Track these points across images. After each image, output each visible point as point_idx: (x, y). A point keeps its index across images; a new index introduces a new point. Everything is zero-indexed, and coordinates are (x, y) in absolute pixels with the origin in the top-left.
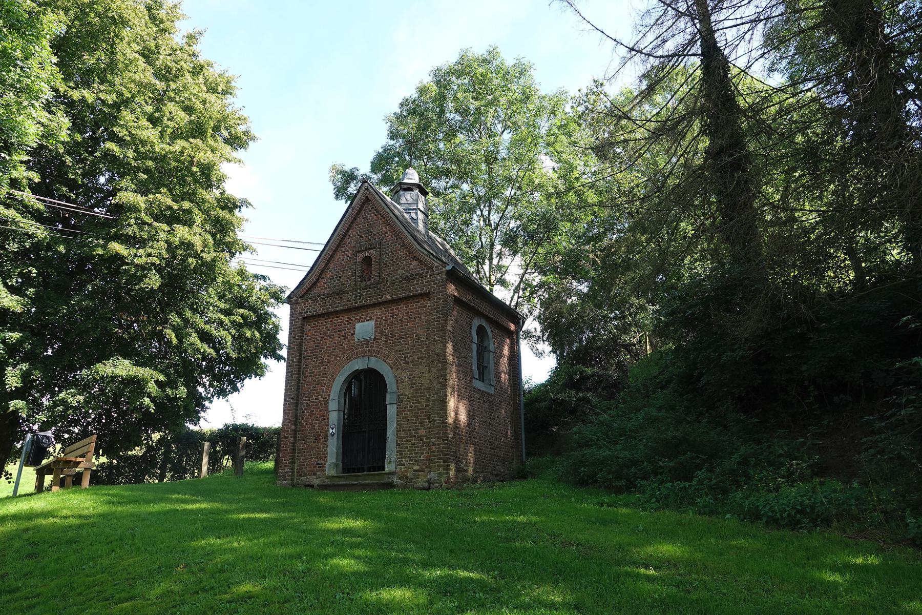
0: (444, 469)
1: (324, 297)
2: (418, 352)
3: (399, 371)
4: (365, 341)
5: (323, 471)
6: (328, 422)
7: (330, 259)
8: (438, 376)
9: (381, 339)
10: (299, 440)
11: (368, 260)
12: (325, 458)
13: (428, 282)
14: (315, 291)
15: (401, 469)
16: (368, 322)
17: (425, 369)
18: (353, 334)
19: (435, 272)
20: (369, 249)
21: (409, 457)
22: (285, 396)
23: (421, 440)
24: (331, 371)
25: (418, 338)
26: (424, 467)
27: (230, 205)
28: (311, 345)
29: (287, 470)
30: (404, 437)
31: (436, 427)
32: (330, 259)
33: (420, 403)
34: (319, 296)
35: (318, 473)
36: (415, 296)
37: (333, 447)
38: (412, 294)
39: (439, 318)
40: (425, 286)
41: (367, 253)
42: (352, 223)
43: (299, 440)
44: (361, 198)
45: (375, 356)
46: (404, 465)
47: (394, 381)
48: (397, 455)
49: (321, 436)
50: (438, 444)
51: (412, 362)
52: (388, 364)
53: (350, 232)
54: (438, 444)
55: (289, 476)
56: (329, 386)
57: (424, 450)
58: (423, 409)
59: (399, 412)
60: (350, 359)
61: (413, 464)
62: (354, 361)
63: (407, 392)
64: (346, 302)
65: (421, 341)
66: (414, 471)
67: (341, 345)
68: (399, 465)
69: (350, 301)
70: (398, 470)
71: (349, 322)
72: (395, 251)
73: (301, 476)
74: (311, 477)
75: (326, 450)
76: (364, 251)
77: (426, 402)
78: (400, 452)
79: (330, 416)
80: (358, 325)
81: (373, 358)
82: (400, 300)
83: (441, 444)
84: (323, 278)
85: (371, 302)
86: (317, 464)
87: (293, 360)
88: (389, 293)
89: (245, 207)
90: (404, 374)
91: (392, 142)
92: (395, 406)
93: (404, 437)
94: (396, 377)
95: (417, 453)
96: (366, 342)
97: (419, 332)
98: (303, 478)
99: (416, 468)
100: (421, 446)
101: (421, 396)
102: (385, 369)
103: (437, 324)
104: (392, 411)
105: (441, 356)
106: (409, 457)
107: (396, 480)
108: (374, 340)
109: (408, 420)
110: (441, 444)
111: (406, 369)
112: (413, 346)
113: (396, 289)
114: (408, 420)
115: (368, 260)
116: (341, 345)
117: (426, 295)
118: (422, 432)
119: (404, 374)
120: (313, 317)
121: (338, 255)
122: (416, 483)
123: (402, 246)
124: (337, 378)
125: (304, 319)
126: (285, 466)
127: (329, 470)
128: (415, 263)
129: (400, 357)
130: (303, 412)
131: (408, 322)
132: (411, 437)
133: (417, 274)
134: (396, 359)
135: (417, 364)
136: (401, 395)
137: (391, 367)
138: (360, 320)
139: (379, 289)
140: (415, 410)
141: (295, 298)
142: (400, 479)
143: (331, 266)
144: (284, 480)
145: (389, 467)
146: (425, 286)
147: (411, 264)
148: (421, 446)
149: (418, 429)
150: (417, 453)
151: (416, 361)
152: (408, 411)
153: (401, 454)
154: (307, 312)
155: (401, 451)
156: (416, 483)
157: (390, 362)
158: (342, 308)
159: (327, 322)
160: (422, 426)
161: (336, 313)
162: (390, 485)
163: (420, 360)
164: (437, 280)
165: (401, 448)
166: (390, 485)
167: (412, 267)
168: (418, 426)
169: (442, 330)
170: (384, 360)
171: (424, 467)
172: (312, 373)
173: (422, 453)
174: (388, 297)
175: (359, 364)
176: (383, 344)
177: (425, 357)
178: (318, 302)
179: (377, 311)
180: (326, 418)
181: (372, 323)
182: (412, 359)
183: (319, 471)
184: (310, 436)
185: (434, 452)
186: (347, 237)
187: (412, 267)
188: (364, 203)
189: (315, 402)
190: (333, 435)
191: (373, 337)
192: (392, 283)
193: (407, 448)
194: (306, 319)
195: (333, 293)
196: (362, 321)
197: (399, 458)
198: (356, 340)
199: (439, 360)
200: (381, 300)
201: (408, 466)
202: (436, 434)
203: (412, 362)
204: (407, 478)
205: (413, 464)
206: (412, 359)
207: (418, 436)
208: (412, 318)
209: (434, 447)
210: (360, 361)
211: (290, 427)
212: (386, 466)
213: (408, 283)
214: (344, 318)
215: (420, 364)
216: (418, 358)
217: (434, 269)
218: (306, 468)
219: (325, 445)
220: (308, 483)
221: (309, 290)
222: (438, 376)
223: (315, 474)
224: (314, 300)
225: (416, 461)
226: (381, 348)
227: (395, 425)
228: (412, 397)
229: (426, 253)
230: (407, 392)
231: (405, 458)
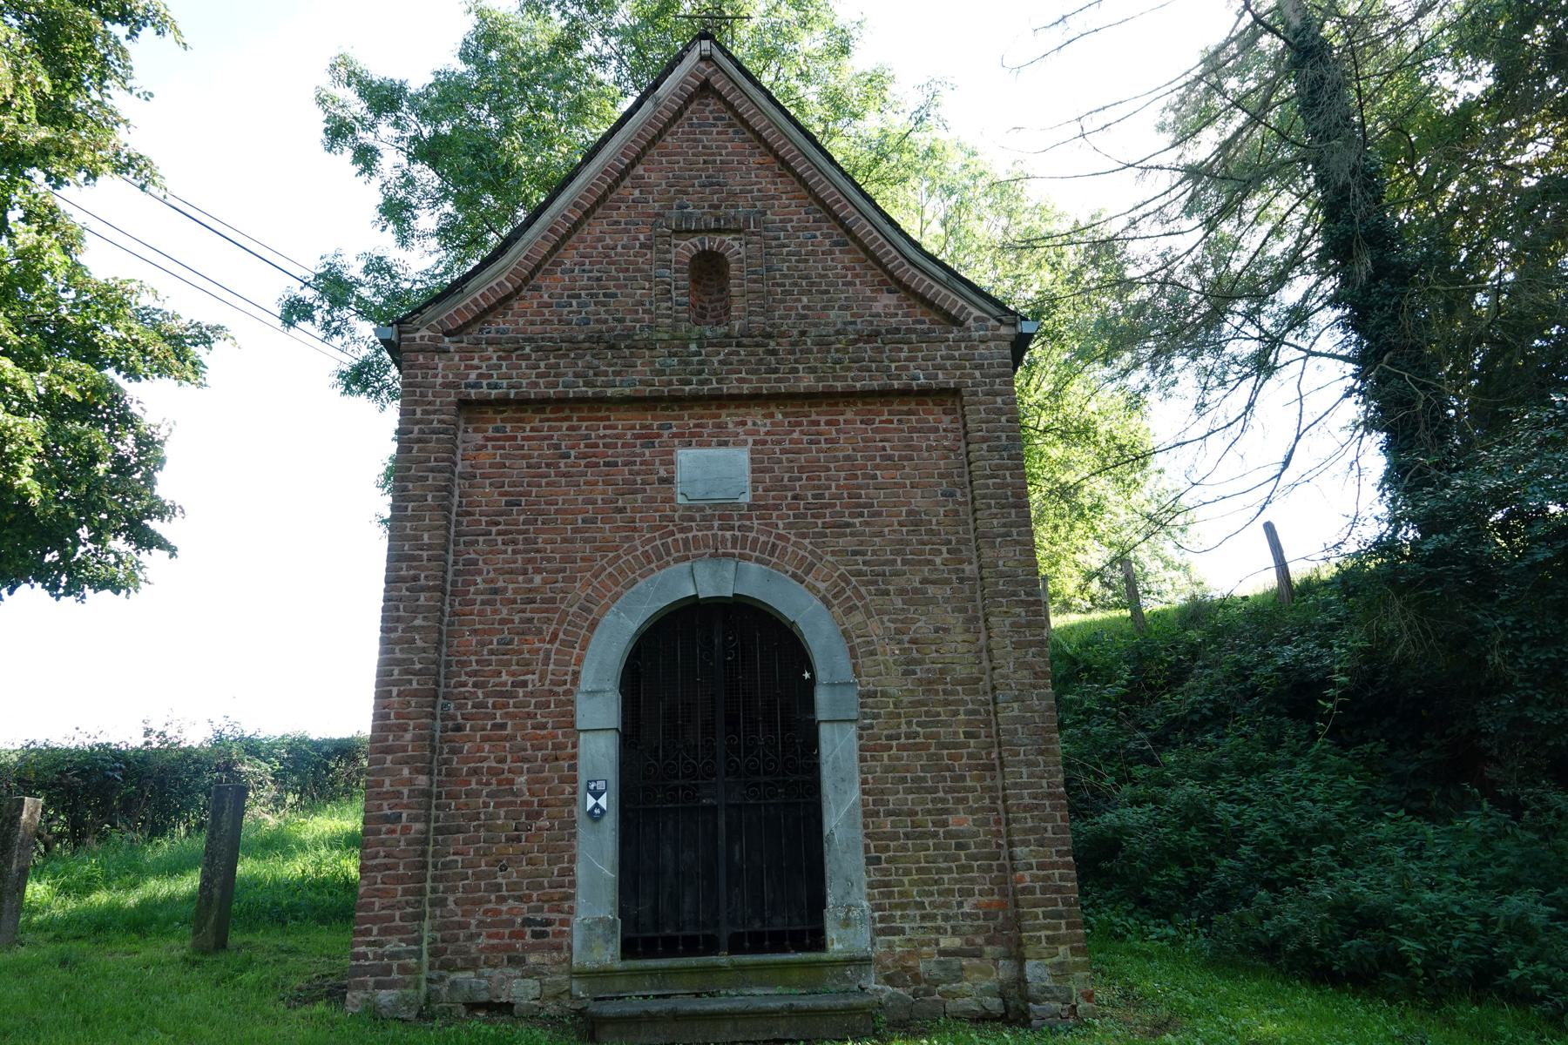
0: (1075, 951)
2: (919, 562)
3: (858, 617)
4: (714, 507)
5: (559, 948)
6: (573, 768)
7: (568, 235)
8: (1018, 645)
9: (776, 507)
10: (438, 831)
11: (709, 268)
12: (563, 895)
13: (952, 358)
14: (502, 324)
15: (890, 945)
16: (722, 451)
17: (954, 620)
18: (668, 481)
19: (975, 335)
20: (718, 231)
21: (921, 905)
23: (959, 847)
24: (579, 591)
25: (915, 520)
26: (979, 940)
28: (487, 495)
29: (394, 944)
30: (895, 836)
31: (1027, 808)
32: (568, 235)
33: (944, 724)
34: (530, 340)
35: (533, 959)
36: (905, 393)
38: (896, 384)
39: (999, 467)
40: (937, 367)
41: (712, 242)
42: (652, 143)
43: (438, 831)
44: (685, 81)
45: (758, 560)
46: (901, 931)
48: (870, 897)
50: (1041, 866)
51: (902, 592)
52: (813, 589)
53: (639, 170)
54: (1041, 866)
55: (404, 969)
56: (575, 642)
57: (972, 881)
58: (956, 746)
59: (869, 750)
60: (659, 558)
61: (938, 930)
62: (674, 567)
63: (894, 684)
64: (640, 376)
65: (931, 532)
66: (943, 953)
67: (621, 510)
68: (882, 932)
69: (661, 373)
71: (648, 439)
72: (813, 253)
73: (449, 966)
74: (497, 974)
75: (570, 871)
76: (697, 231)
77: (968, 723)
78: (882, 886)
79: (581, 750)
80: (686, 458)
81: (753, 566)
82: (850, 396)
83: (1053, 865)
84: (537, 288)
85: (746, 389)
86: (527, 922)
87: (418, 538)
88: (813, 370)
90: (874, 627)
92: (852, 730)
93: (895, 836)
94: (846, 634)
95: (950, 892)
96: (724, 512)
97: (918, 502)
98: (459, 976)
99: (945, 942)
101: (947, 703)
103: (997, 486)
105: (1023, 583)
106: (921, 905)
108: (751, 507)
109: (904, 780)
110: (1053, 865)
111: (880, 612)
112: (900, 542)
113: (839, 361)
114: (904, 780)
115: (709, 268)
116: (621, 510)
117: (947, 396)
118: (961, 821)
119: (874, 627)
120: (502, 403)
121: (594, 229)
122: (954, 995)
123: (836, 244)
124: (609, 617)
125: (464, 404)
126: (383, 932)
127: (587, 946)
129: (859, 573)
130: (459, 728)
131: (877, 467)
132: (922, 836)
133: (909, 331)
135: (915, 598)
136: (873, 694)
137: (824, 600)
138: (690, 439)
139: (774, 353)
140: (926, 747)
141: (425, 332)
142: (889, 980)
143: (569, 258)
144: (380, 985)
145: (838, 943)
146: (937, 367)
147: (875, 300)
148: (963, 869)
149: (946, 811)
150: (950, 892)
151: (915, 591)
152: (901, 748)
153: (890, 895)
154: (477, 385)
155: (887, 884)
156: (954, 995)
157: (822, 586)
158: (627, 391)
160: (959, 801)
161: (597, 404)
163: (931, 590)
164: (982, 357)
165: (886, 872)
167: (878, 307)
168: (943, 800)
169: (1015, 506)
170: (794, 576)
171: (979, 940)
172: (495, 591)
173: (970, 893)
174: (806, 382)
176: (789, 526)
177: (947, 582)
178: (528, 357)
179: (757, 419)
180: (564, 755)
181: (741, 457)
182: (901, 582)
183: (533, 949)
184: (491, 817)
185: (1031, 891)
186: (627, 182)
187: (878, 307)
188: (690, 99)
189: (512, 695)
190: (595, 816)
191: (746, 499)
192: (823, 344)
193: (907, 872)
194: (469, 407)
195: (589, 339)
196: (700, 445)
197: (878, 907)
198: (680, 499)
199: (1014, 594)
200: (783, 387)
201: (919, 936)
202: (1032, 830)
203: (902, 592)
204: (917, 978)
205: (938, 930)
206: (901, 582)
207: (948, 835)
208: (890, 458)
209: (1027, 875)
210: (703, 570)
211: (410, 782)
212: (832, 932)
214: (625, 425)
216: (924, 581)
217: (970, 322)
218: (471, 937)
219: (562, 848)
220: (484, 997)
221: (482, 316)
222: (1018, 645)
224: (511, 349)
225: (946, 918)
226: (779, 537)
227: (855, 795)
229: (942, 275)
230: (894, 684)
231: (903, 907)
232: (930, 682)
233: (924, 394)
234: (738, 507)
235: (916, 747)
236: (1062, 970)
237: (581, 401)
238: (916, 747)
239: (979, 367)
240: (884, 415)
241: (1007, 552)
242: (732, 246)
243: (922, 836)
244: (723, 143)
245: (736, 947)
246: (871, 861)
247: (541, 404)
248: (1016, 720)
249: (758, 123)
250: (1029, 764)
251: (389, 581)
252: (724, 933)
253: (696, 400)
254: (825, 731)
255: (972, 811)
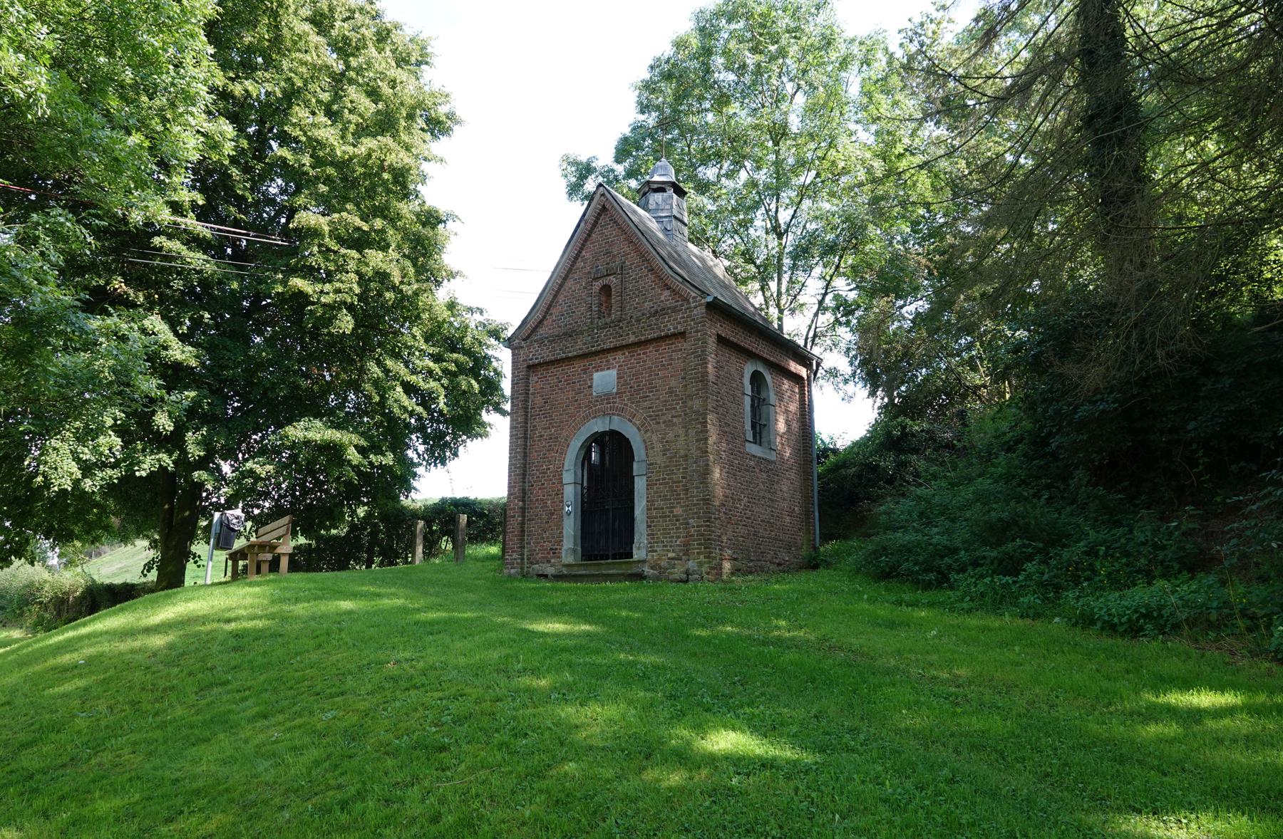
0: (705, 557)
1: (554, 339)
3: (649, 434)
8: (697, 441)
12: (560, 542)
17: (681, 431)
18: (590, 387)
19: (692, 305)
20: (608, 275)
22: (510, 465)
23: (677, 520)
24: (565, 433)
25: (671, 391)
27: (431, 219)
29: (515, 556)
30: (656, 517)
31: (695, 505)
36: (667, 336)
37: (570, 528)
38: (663, 334)
40: (679, 323)
41: (606, 281)
42: (586, 240)
44: (596, 208)
47: (643, 446)
49: (555, 515)
51: (664, 422)
52: (635, 424)
53: (583, 253)
60: (587, 418)
63: (659, 460)
64: (580, 346)
65: (676, 395)
69: (585, 344)
70: (649, 557)
75: (561, 532)
78: (651, 535)
80: (596, 376)
81: (616, 417)
83: (702, 526)
88: (634, 333)
89: (451, 221)
90: (654, 438)
91: (642, 117)
92: (645, 478)
93: (656, 517)
96: (607, 397)
97: (673, 383)
100: (678, 528)
102: (630, 431)
103: (696, 373)
104: (640, 484)
107: (647, 570)
108: (617, 394)
110: (702, 526)
115: (606, 290)
117: (682, 335)
118: (678, 511)
120: (540, 364)
121: (569, 283)
122: (672, 573)
124: (572, 443)
125: (529, 367)
127: (566, 557)
128: (667, 293)
129: (651, 416)
132: (665, 517)
133: (669, 308)
134: (645, 419)
135: (669, 424)
136: (652, 464)
137: (638, 429)
139: (621, 328)
140: (668, 483)
142: (652, 568)
143: (561, 298)
145: (638, 554)
146: (679, 323)
148: (678, 528)
152: (661, 484)
156: (672, 573)
157: (638, 423)
159: (557, 371)
162: (640, 577)
163: (675, 420)
166: (640, 577)
167: (663, 298)
174: (632, 339)
175: (599, 425)
177: (680, 416)
179: (620, 357)
180: (560, 493)
183: (553, 558)
185: (693, 535)
186: (580, 259)
187: (663, 298)
188: (599, 215)
190: (569, 514)
191: (615, 390)
192: (638, 321)
195: (564, 334)
196: (602, 370)
200: (624, 343)
204: (660, 568)
206: (664, 418)
207: (674, 516)
210: (599, 421)
212: (634, 552)
213: (657, 320)
214: (578, 366)
215: (674, 425)
216: (673, 417)
217: (691, 300)
219: (560, 526)
221: (534, 330)
222: (697, 441)
223: (549, 561)
224: (541, 342)
228: (665, 467)
229: (680, 280)
230: (659, 460)
232: (672, 458)
233: (675, 335)
234: (612, 394)
235: (665, 483)
236: (700, 564)
237: (563, 360)
238: (665, 483)
239: (693, 320)
240: (663, 346)
241: (697, 402)
242: (612, 280)
243: (665, 517)
244: (611, 231)
245: (614, 558)
246: (649, 526)
247: (552, 362)
248: (694, 471)
249: (620, 221)
250: (697, 488)
251: (511, 436)
252: (610, 553)
253: (596, 353)
254: (636, 479)
255: (682, 507)
